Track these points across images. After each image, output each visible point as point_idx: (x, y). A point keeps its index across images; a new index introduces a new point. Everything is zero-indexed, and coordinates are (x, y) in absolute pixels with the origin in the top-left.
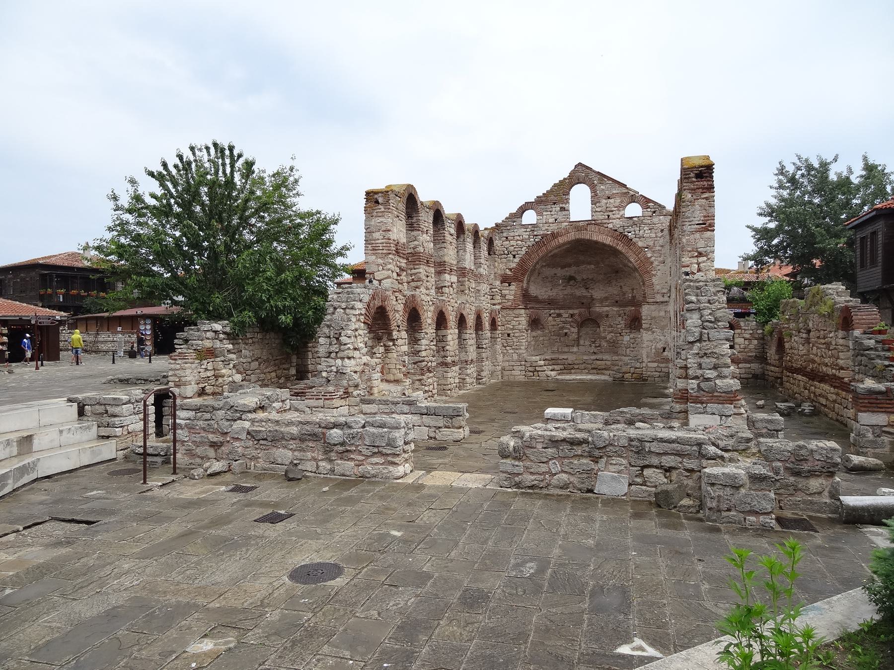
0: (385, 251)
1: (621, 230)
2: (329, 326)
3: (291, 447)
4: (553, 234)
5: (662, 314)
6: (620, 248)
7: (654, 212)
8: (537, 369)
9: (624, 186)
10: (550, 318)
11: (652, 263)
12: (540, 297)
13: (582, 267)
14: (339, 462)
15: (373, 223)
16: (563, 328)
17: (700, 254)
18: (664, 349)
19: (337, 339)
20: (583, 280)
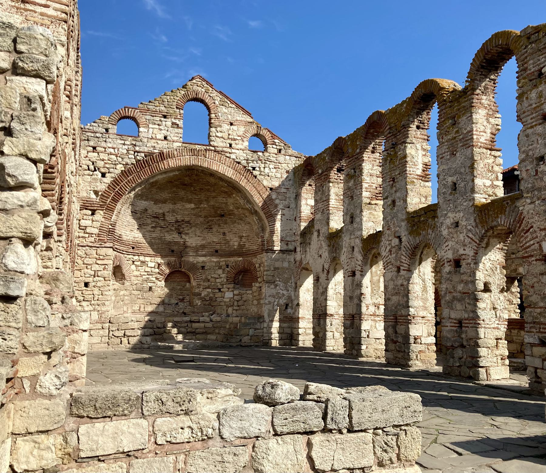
1: (244, 162)
4: (161, 154)
5: (286, 265)
6: (243, 183)
8: (128, 333)
10: (133, 267)
11: (276, 206)
12: (125, 238)
13: (179, 206)
16: (147, 280)
18: (287, 305)
20: (177, 221)
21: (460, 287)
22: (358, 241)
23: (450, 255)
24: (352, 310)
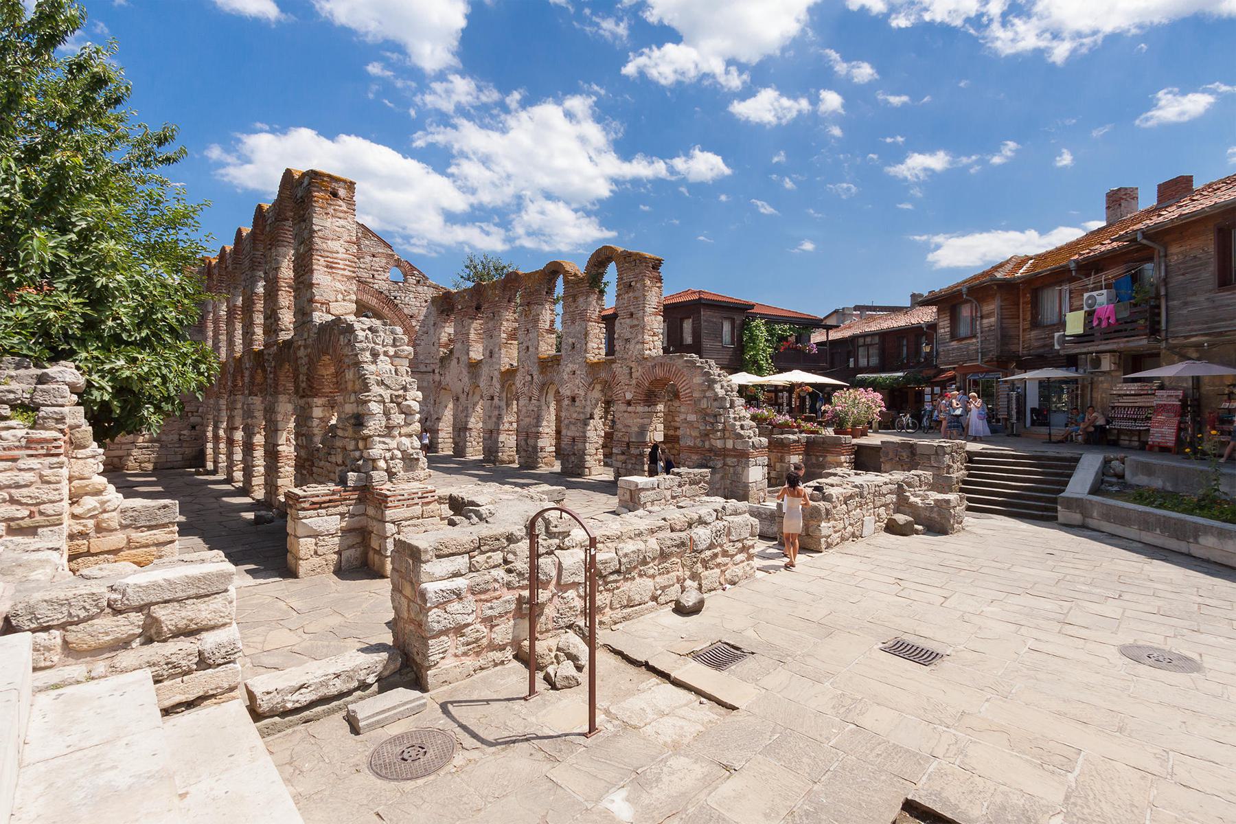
0: (347, 273)
1: (386, 292)
2: (381, 383)
3: (651, 572)
7: (418, 282)
9: (390, 247)
14: (706, 573)
15: (328, 224)
17: (654, 335)
19: (399, 404)
21: (575, 415)
22: (496, 373)
23: (569, 393)
24: (491, 426)
